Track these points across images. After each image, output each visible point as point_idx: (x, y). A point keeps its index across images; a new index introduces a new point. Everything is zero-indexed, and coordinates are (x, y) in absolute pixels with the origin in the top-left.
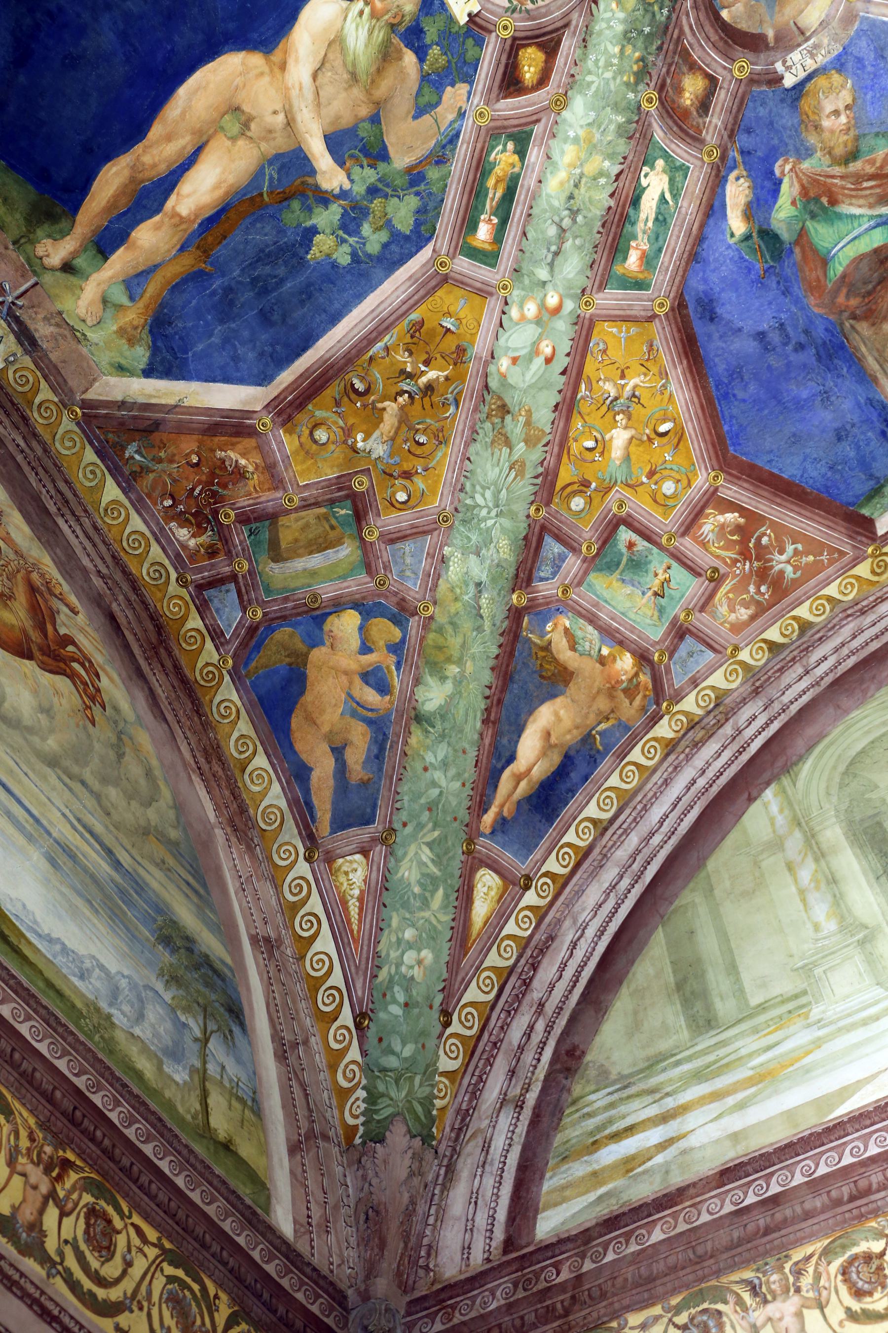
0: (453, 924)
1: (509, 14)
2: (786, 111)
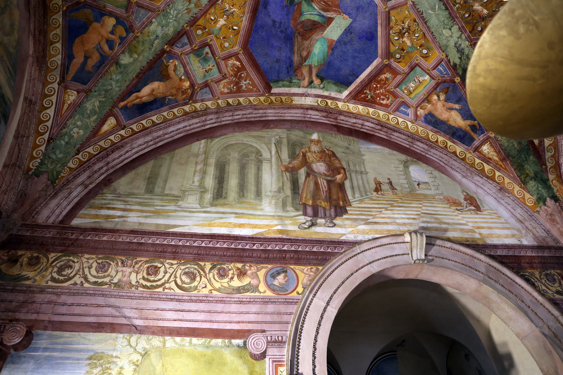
0: (95, 128)
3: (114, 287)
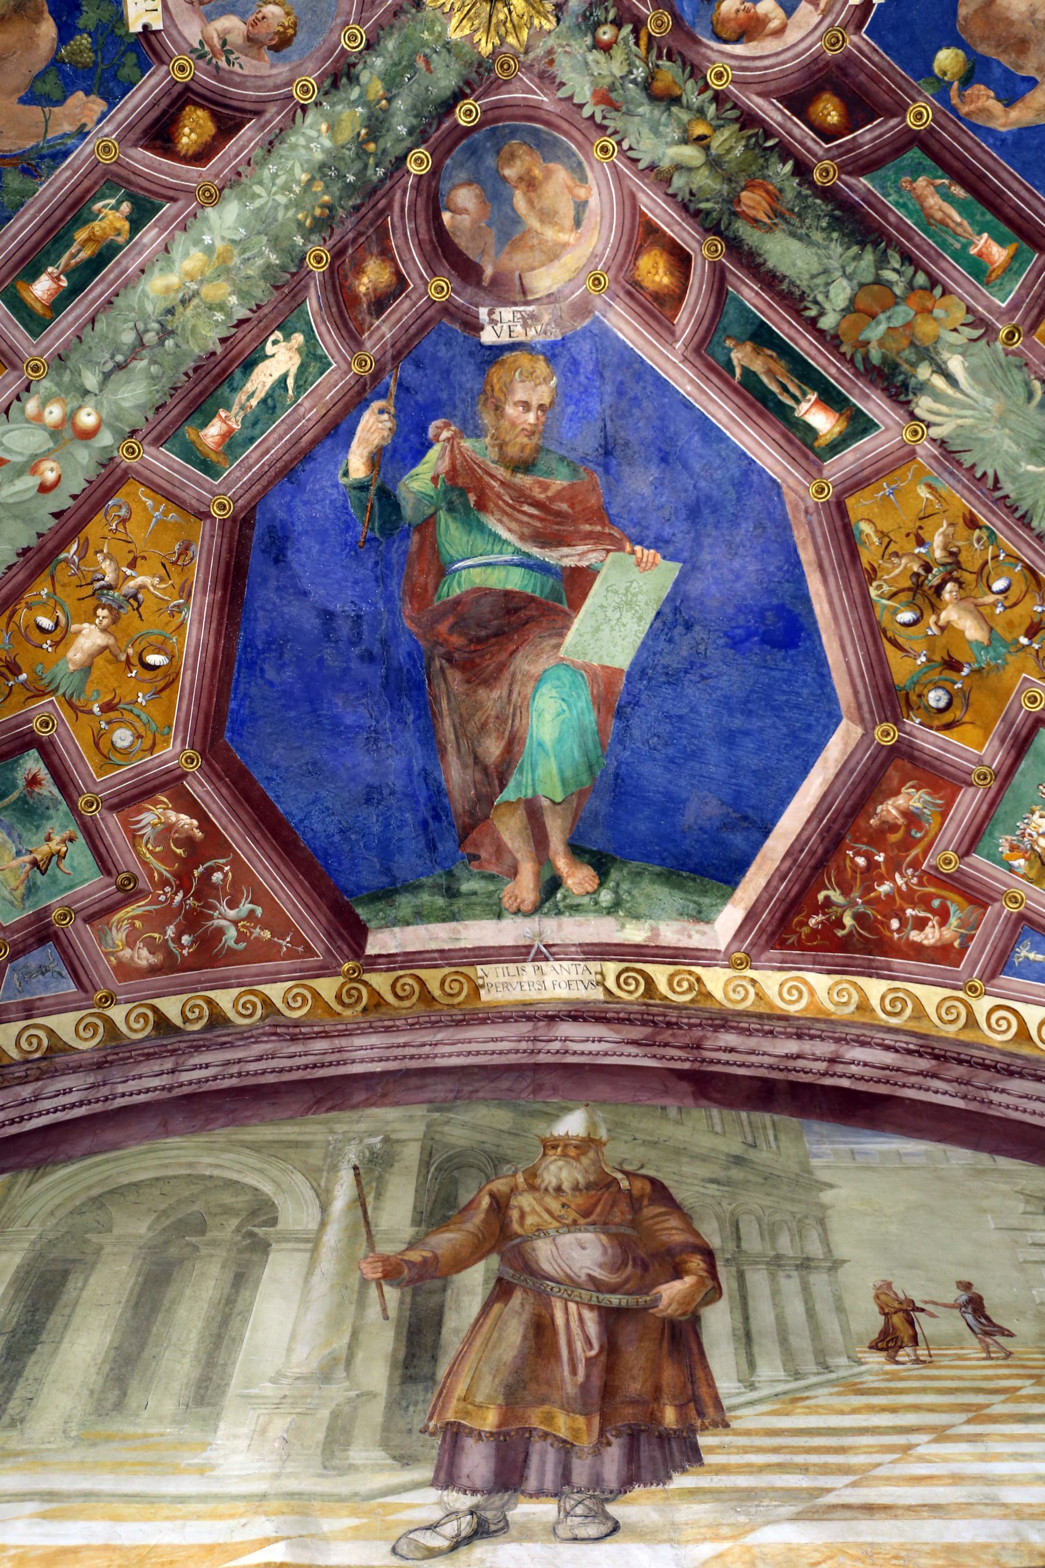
1: (194, 56)
2: (471, 368)
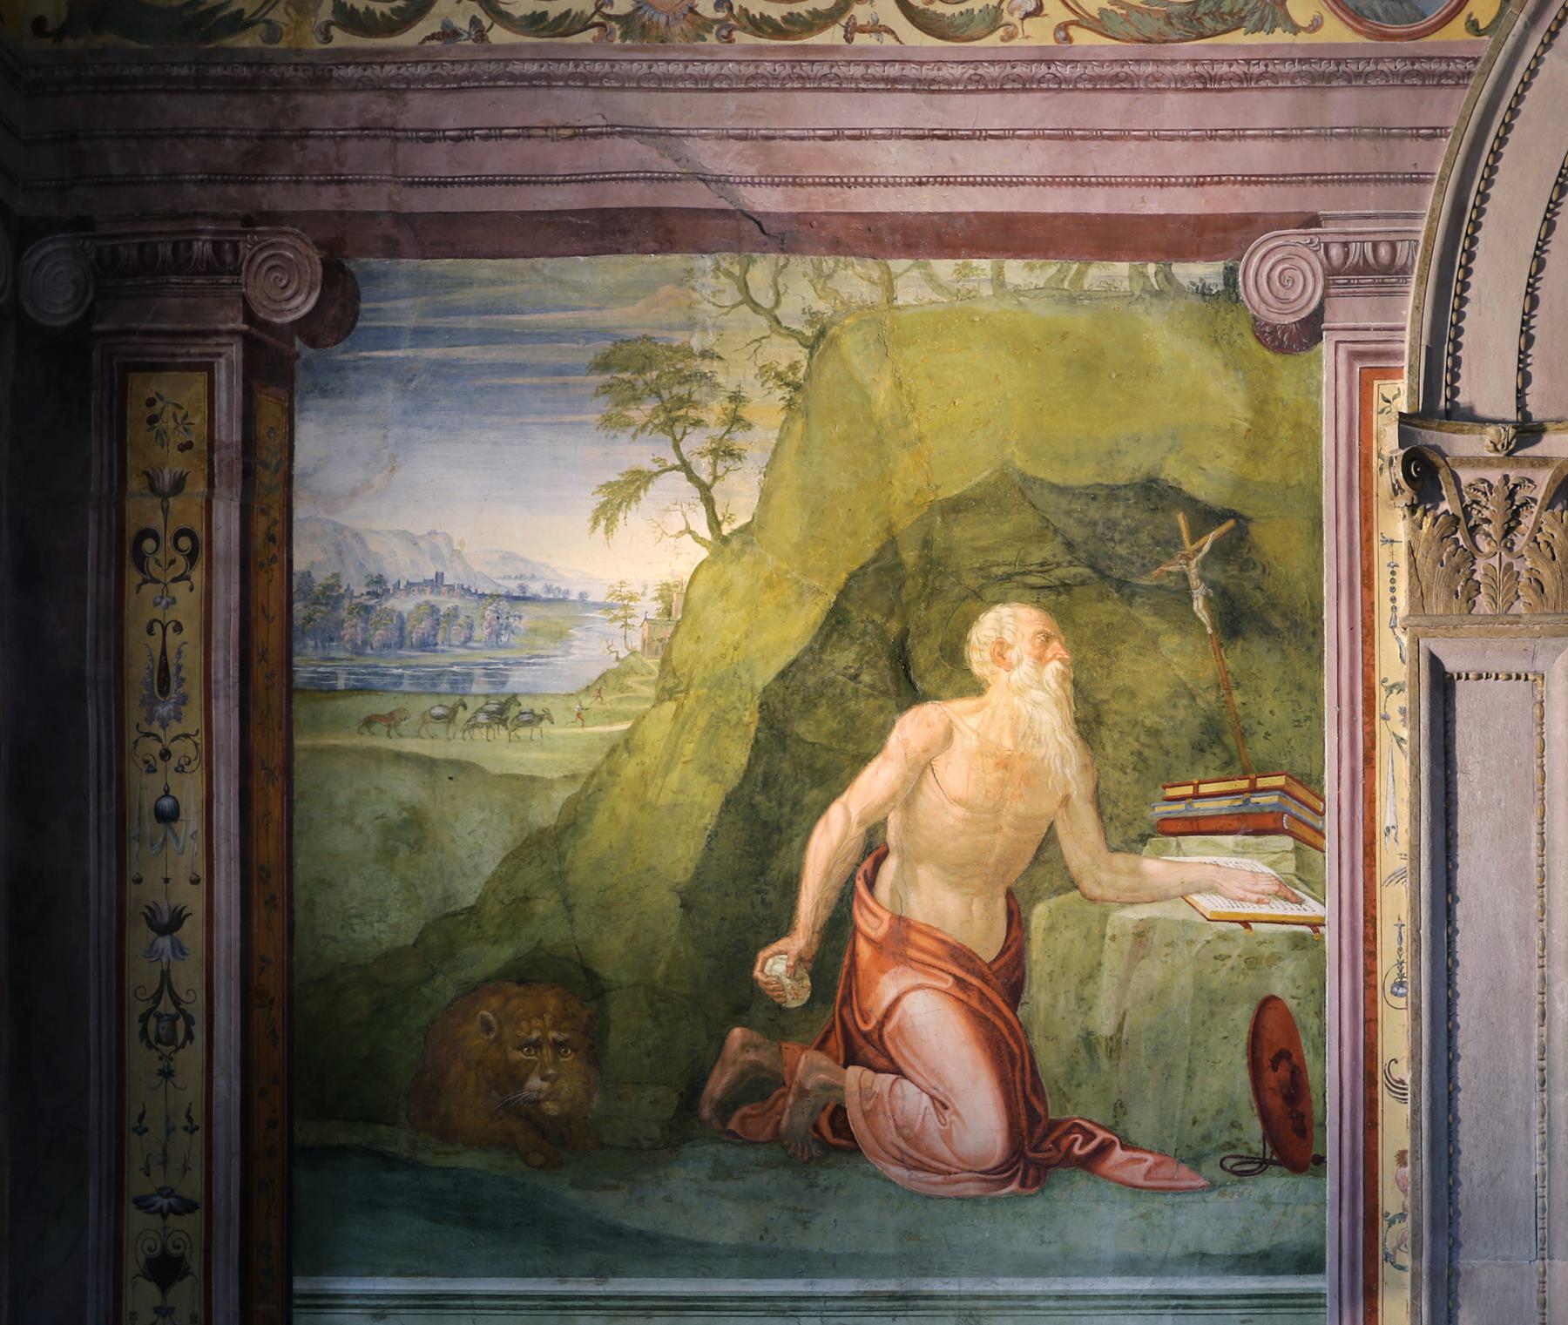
3: (624, 36)
